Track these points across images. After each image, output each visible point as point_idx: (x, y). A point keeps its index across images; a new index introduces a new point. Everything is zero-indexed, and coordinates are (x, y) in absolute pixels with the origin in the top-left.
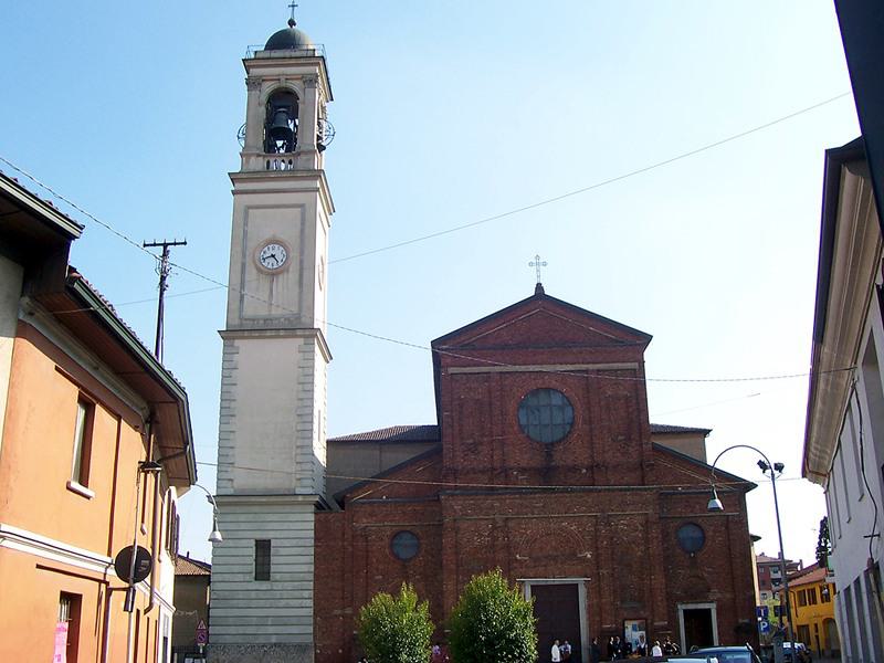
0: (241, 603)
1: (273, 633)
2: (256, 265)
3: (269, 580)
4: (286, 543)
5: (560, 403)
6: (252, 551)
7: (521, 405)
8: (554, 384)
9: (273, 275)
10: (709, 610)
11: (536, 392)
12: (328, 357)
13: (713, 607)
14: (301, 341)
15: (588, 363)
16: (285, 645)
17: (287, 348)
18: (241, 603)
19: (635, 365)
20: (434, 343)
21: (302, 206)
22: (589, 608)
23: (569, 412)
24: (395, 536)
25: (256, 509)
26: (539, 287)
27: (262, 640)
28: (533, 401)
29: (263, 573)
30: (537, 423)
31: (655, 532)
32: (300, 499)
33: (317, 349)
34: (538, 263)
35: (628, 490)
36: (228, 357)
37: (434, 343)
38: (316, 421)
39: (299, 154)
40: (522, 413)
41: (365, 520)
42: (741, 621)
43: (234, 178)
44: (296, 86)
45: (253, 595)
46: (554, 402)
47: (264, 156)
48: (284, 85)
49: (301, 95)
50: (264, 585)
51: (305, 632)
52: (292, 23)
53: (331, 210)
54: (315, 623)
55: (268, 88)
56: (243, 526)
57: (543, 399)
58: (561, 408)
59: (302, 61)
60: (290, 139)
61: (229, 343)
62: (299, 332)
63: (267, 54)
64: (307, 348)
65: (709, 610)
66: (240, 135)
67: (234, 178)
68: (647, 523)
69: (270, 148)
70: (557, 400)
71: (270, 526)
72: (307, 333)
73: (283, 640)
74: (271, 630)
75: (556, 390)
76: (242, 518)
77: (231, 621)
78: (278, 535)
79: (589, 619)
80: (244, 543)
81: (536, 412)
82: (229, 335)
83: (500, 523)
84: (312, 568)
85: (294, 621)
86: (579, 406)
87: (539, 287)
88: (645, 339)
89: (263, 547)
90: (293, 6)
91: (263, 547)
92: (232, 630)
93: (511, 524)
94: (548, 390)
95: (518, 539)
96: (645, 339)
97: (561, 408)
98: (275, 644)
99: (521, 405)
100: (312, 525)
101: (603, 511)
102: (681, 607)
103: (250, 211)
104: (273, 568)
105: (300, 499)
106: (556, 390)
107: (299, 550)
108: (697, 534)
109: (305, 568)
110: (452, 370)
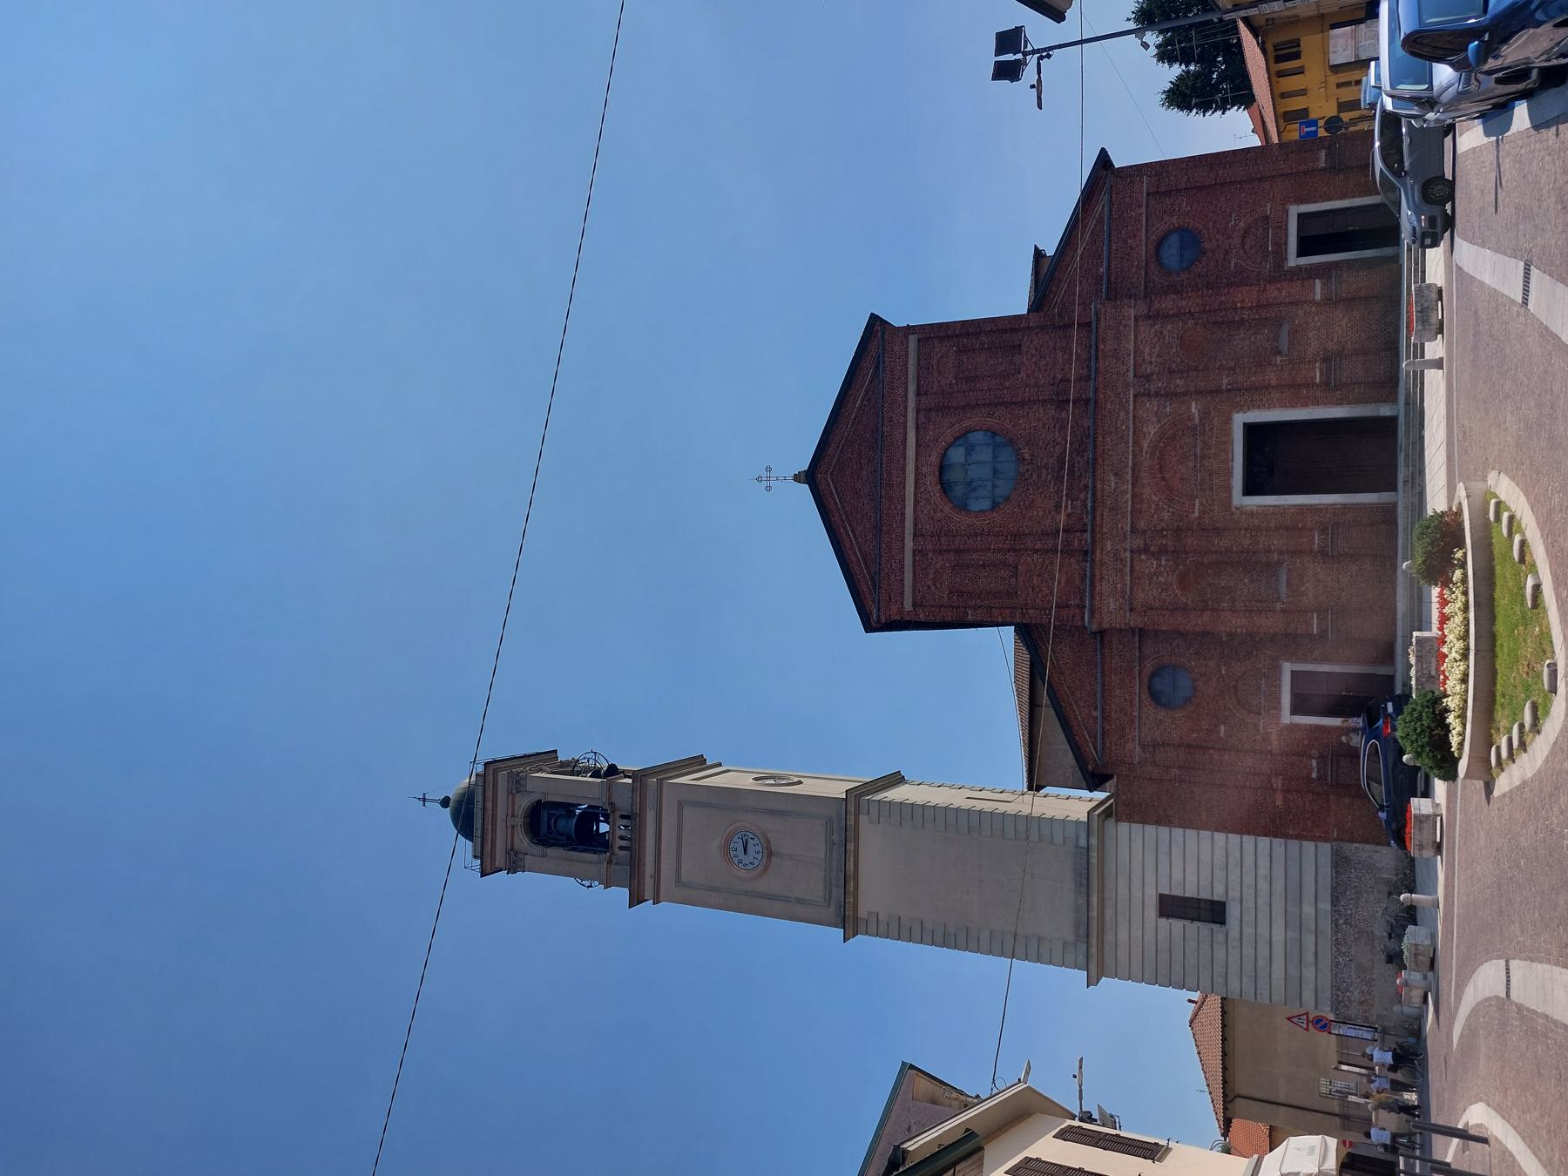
0: (1263, 951)
1: (1316, 908)
2: (760, 875)
3: (1225, 903)
4: (1164, 869)
5: (962, 450)
6: (1178, 925)
7: (963, 507)
8: (934, 459)
9: (770, 854)
10: (1300, 216)
11: (945, 487)
12: (896, 779)
13: (1294, 210)
14: (863, 819)
15: (906, 408)
16: (1334, 889)
17: (873, 846)
18: (1263, 951)
19: (913, 339)
20: (869, 627)
21: (680, 805)
22: (1293, 405)
23: (977, 437)
24: (1155, 696)
25: (1109, 912)
26: (797, 478)
27: (1326, 926)
28: (959, 490)
29: (1215, 912)
30: (989, 485)
31: (1167, 304)
32: (1094, 841)
33: (878, 797)
34: (766, 478)
35: (1097, 346)
36: (883, 928)
37: (869, 627)
38: (979, 805)
39: (612, 804)
40: (975, 506)
41: (1129, 746)
42: (1322, 164)
43: (636, 899)
44: (523, 803)
45: (1249, 931)
46: (962, 459)
47: (613, 854)
48: (519, 821)
49: (535, 797)
50: (1233, 912)
51: (1314, 857)
52: (445, 802)
53: (698, 762)
54: (1299, 837)
55: (523, 841)
56: (1137, 933)
57: (955, 475)
58: (970, 449)
59: (489, 794)
60: (592, 816)
61: (862, 927)
62: (851, 822)
63: (479, 840)
64: (874, 810)
65: (1300, 216)
66: (587, 883)
67: (636, 899)
68: (1154, 317)
69: (600, 844)
70: (957, 455)
71: (1137, 893)
72: (852, 808)
73: (1326, 894)
74: (1308, 909)
75: (944, 456)
76: (1123, 935)
77: (1293, 971)
78: (1150, 879)
79: (1305, 405)
80: (1162, 935)
81: (974, 484)
82: (850, 923)
83: (1139, 542)
84: (1205, 834)
85: (1294, 873)
86: (966, 423)
87: (797, 478)
88: (875, 322)
89: (1172, 907)
90: (424, 800)
91: (1172, 907)
92: (1309, 973)
93: (1142, 525)
94: (942, 468)
95: (1166, 515)
96: (875, 322)
97: (970, 449)
98: (1335, 901)
99: (963, 507)
100: (1136, 827)
101: (1127, 386)
102: (1293, 260)
103: (684, 879)
104: (1205, 895)
105: (1094, 841)
106: (944, 456)
107: (1176, 851)
108: (1174, 240)
109: (1206, 845)
110: (908, 606)
